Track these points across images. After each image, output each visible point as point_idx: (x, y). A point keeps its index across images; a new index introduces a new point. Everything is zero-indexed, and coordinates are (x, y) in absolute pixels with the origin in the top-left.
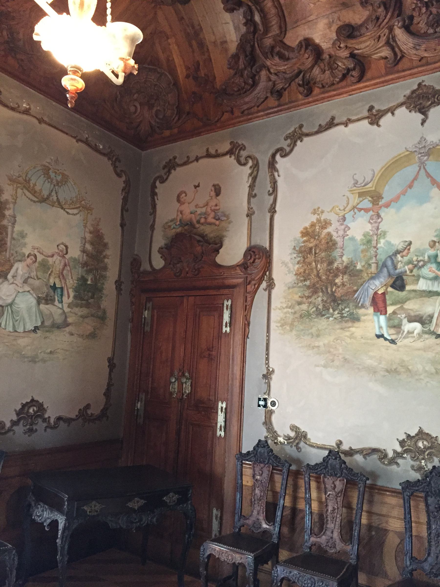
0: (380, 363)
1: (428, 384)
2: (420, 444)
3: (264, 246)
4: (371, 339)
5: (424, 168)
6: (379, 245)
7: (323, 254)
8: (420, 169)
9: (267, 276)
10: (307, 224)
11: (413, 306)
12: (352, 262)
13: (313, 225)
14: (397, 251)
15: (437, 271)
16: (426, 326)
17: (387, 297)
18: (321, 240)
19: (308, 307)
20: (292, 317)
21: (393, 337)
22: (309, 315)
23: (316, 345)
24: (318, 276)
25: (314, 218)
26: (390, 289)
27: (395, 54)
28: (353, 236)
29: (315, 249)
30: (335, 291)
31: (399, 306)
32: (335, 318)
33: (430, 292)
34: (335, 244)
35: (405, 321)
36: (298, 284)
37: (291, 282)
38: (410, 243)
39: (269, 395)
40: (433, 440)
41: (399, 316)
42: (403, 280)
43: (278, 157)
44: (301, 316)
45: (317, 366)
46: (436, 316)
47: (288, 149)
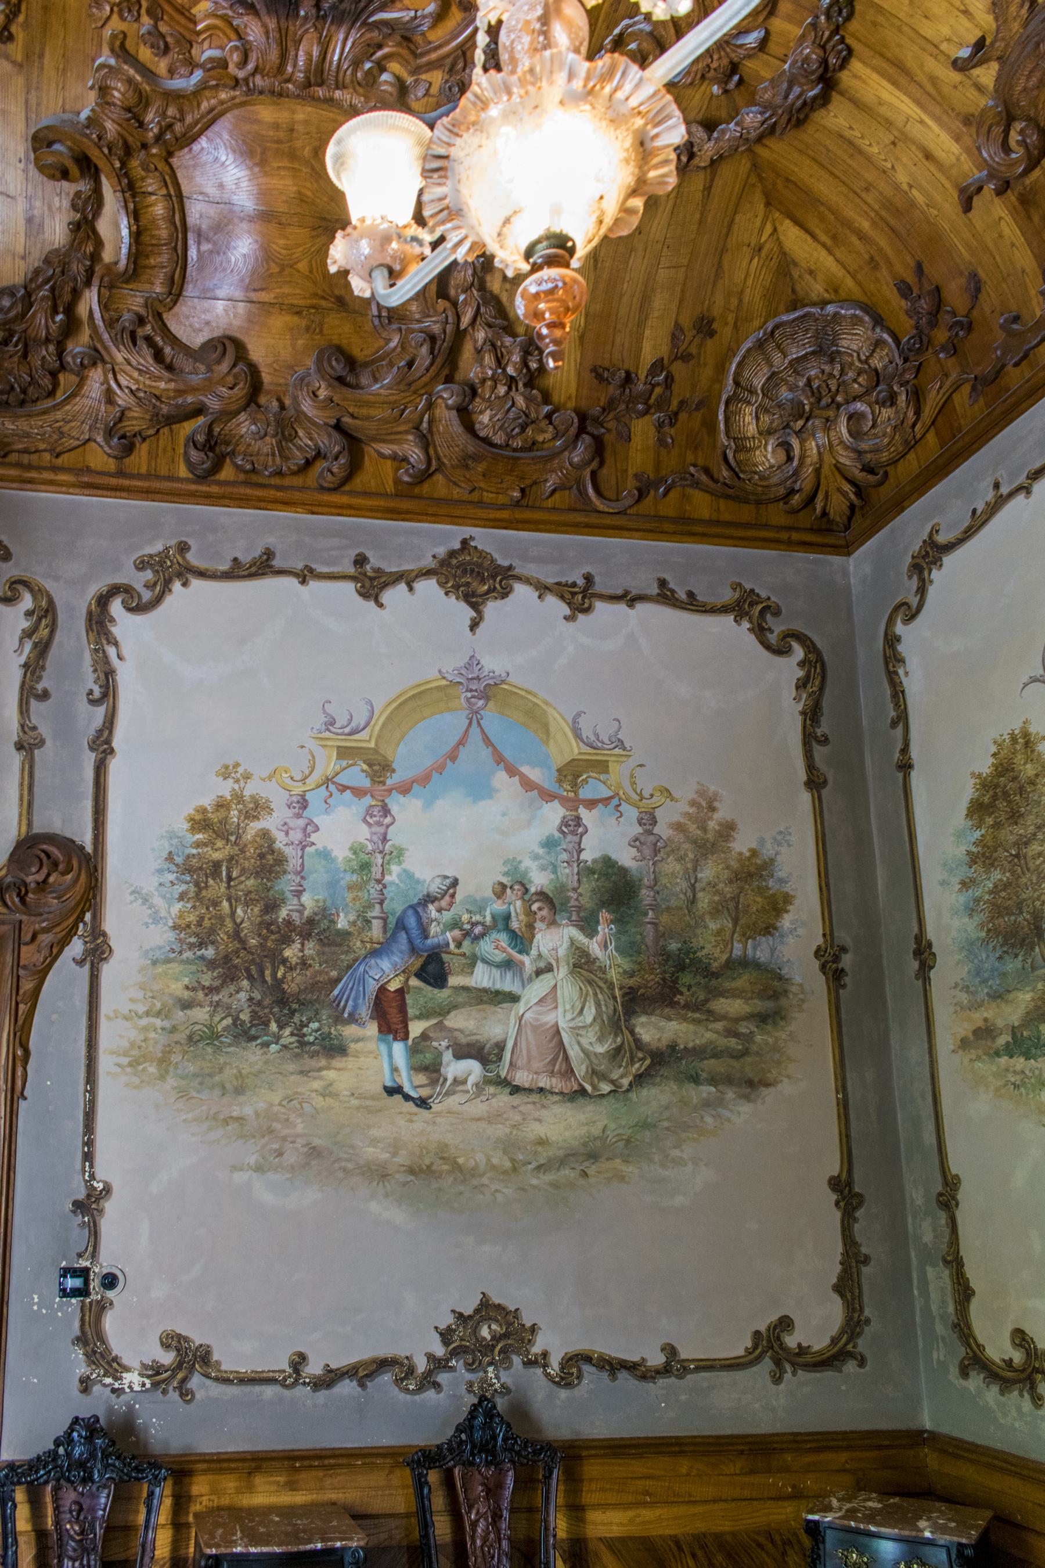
0: (395, 1154)
1: (499, 1196)
2: (485, 1332)
3: (78, 840)
4: (373, 1098)
5: (479, 723)
6: (388, 878)
7: (251, 882)
8: (470, 723)
9: (85, 924)
10: (207, 801)
11: (463, 1022)
12: (325, 909)
13: (221, 805)
14: (428, 895)
15: (509, 950)
16: (492, 1067)
17: (409, 1000)
18: (246, 845)
19: (212, 1016)
20: (163, 1039)
21: (424, 1092)
22: (212, 1036)
23: (235, 1114)
24: (236, 934)
25: (225, 789)
26: (414, 982)
28: (325, 848)
29: (228, 868)
30: (284, 977)
31: (434, 1021)
32: (285, 1046)
33: (497, 993)
34: (281, 860)
35: (448, 1056)
36: (180, 952)
37: (160, 948)
38: (455, 883)
39: (94, 1255)
40: (511, 1318)
41: (435, 1044)
42: (442, 963)
43: (116, 607)
44: (190, 1038)
45: (234, 1168)
46: (510, 1045)
47: (147, 595)
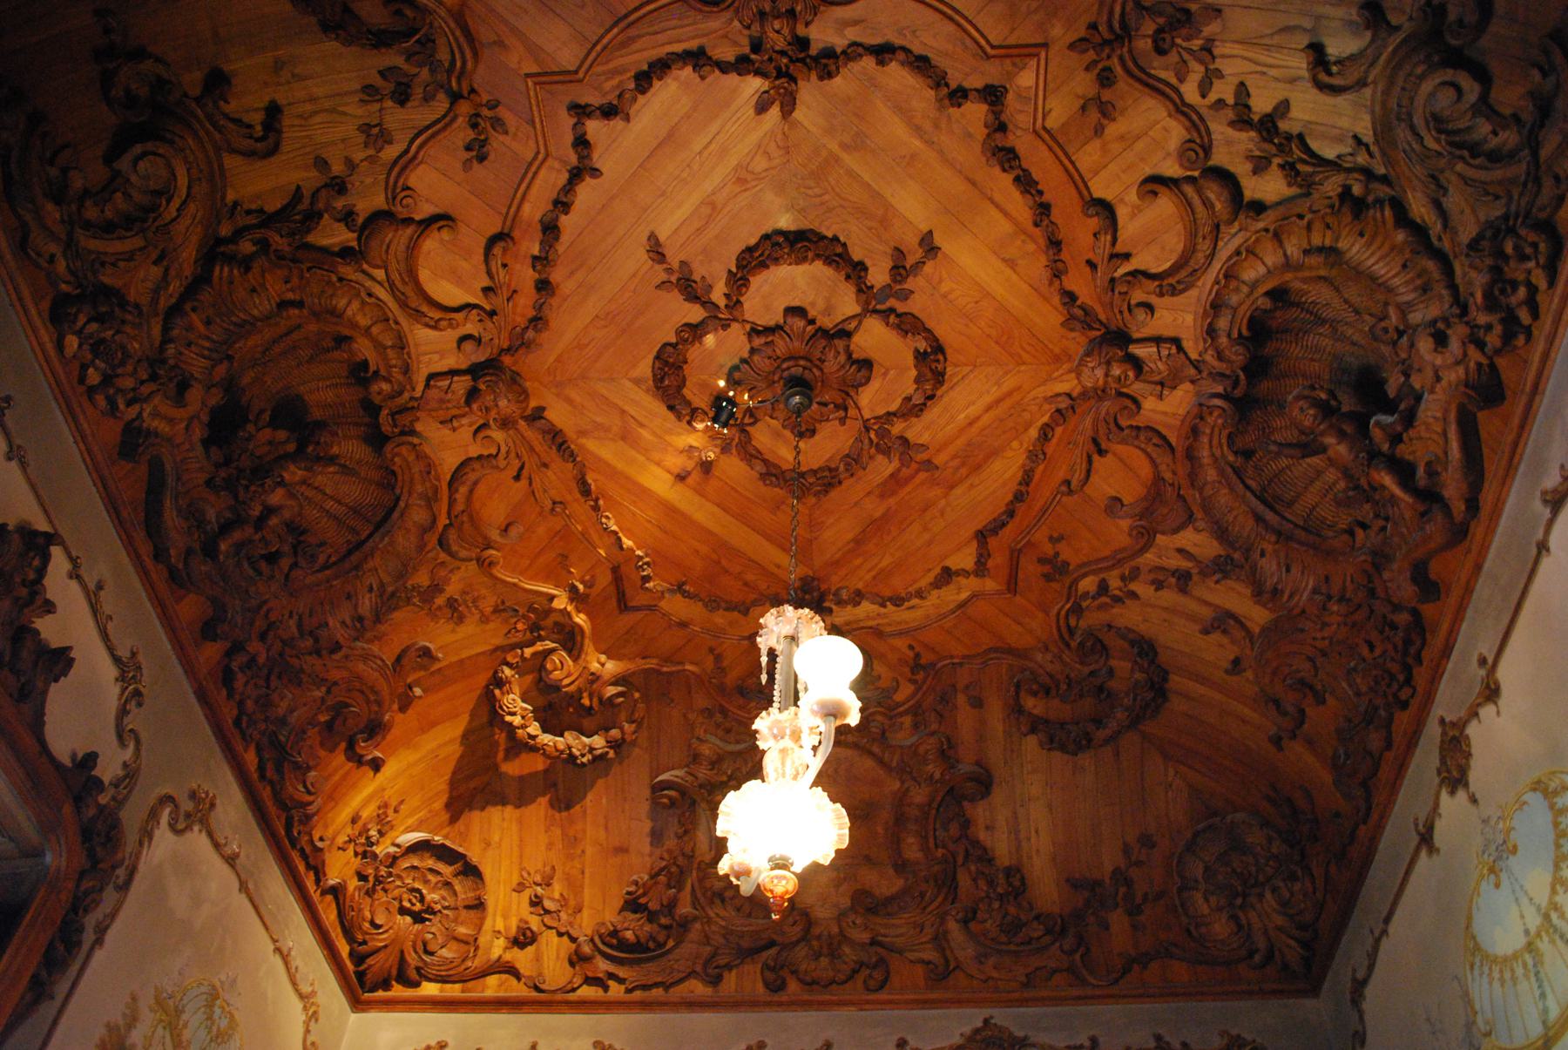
27: (947, 961)
